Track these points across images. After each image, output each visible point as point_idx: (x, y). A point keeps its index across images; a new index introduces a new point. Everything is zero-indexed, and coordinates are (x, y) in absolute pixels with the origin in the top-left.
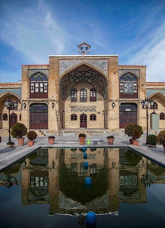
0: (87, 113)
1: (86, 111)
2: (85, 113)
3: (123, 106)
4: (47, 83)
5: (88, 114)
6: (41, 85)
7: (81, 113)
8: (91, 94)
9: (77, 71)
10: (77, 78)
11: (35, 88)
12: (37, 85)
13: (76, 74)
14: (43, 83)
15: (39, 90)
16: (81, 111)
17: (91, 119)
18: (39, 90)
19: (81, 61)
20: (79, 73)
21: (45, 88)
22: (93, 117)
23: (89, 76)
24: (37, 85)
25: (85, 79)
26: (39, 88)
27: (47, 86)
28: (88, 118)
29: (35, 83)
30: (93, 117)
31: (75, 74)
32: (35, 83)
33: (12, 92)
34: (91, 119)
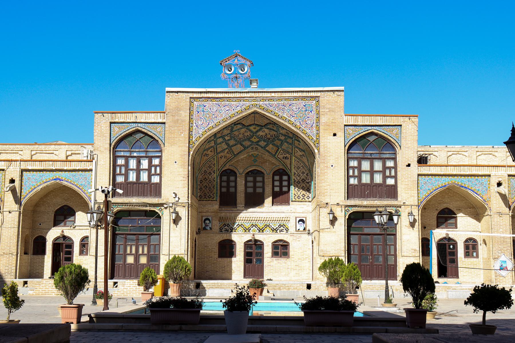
0: (265, 236)
1: (261, 230)
2: (258, 237)
3: (356, 219)
4: (160, 157)
5: (268, 240)
6: (145, 164)
7: (248, 237)
8: (277, 183)
9: (237, 124)
10: (236, 141)
11: (127, 169)
12: (133, 164)
13: (236, 133)
14: (150, 159)
15: (138, 177)
16: (247, 230)
17: (275, 254)
18: (138, 177)
19: (248, 104)
20: (243, 130)
21: (153, 172)
22: (281, 249)
23: (269, 136)
24: (133, 164)
25: (260, 143)
26: (138, 170)
27: (160, 165)
28: (268, 250)
29: (127, 158)
30: (281, 249)
31: (232, 131)
32: (127, 158)
33: (69, 180)
34: (275, 254)
